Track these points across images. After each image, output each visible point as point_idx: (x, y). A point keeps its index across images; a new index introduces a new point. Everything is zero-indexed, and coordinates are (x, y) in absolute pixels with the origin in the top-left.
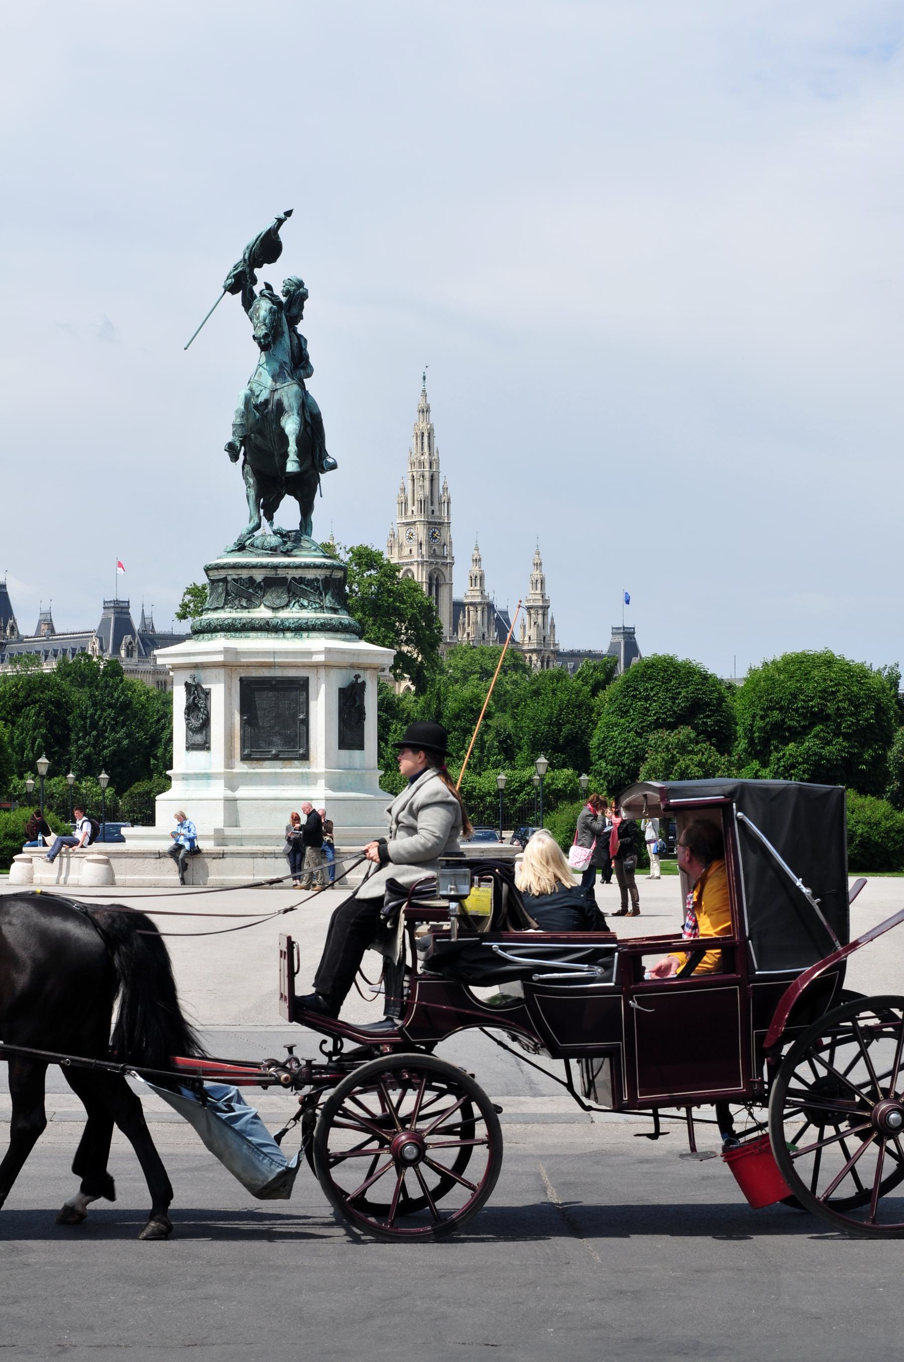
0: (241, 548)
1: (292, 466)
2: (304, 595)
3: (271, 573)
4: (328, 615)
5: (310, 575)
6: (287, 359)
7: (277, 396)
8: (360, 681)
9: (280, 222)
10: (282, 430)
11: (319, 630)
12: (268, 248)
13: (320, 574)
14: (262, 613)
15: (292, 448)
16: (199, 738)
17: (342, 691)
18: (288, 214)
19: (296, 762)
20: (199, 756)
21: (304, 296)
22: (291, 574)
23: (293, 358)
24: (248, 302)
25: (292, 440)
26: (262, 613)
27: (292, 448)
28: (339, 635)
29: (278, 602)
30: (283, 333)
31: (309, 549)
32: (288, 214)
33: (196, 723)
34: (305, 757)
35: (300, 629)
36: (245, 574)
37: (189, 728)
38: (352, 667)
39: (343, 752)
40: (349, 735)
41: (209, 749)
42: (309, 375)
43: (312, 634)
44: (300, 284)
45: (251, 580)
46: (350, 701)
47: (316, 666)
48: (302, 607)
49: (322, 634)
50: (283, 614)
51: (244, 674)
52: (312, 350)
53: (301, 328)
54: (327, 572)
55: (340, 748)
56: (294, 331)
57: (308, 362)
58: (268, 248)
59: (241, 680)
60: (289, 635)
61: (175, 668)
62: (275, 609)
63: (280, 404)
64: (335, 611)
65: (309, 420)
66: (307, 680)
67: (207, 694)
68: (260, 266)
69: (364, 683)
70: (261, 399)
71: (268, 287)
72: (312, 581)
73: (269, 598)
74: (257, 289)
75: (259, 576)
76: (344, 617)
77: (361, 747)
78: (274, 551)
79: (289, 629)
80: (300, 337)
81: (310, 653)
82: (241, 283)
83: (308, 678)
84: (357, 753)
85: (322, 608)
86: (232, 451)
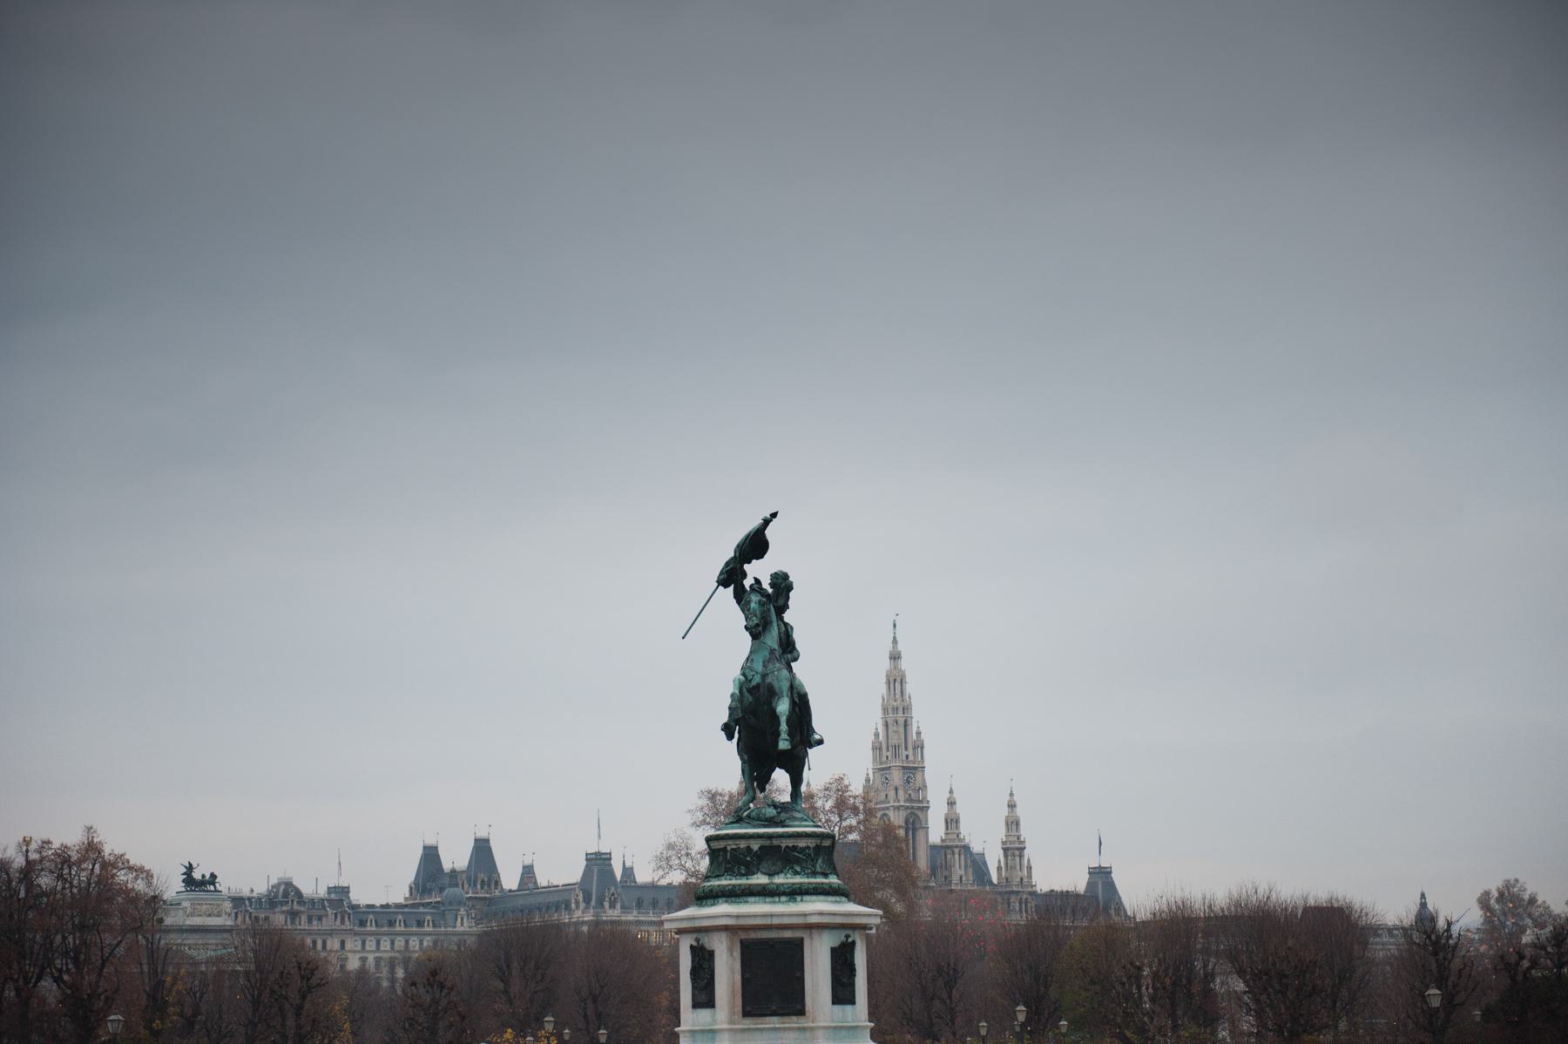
0: (739, 820)
1: (783, 745)
2: (798, 861)
3: (767, 843)
4: (820, 880)
5: (802, 843)
6: (776, 646)
7: (769, 680)
9: (766, 522)
10: (774, 711)
12: (755, 545)
13: (811, 843)
14: (760, 879)
15: (784, 727)
16: (703, 998)
17: (833, 950)
18: (774, 515)
20: (704, 1015)
21: (790, 588)
22: (784, 843)
23: (781, 645)
24: (740, 595)
25: (783, 720)
26: (760, 879)
27: (784, 727)
28: (830, 898)
31: (802, 819)
32: (774, 515)
33: (703, 984)
34: (801, 1012)
35: (794, 893)
36: (743, 844)
37: (694, 988)
38: (843, 926)
39: (837, 1007)
40: (842, 993)
41: (713, 1006)
42: (795, 659)
43: (806, 898)
44: (785, 576)
45: (749, 849)
46: (842, 960)
47: (810, 927)
48: (796, 873)
49: (814, 898)
50: (779, 880)
51: (744, 936)
52: (796, 636)
53: (787, 617)
56: (782, 619)
57: (794, 648)
58: (755, 545)
59: (742, 942)
60: (783, 899)
61: (680, 931)
62: (770, 875)
64: (825, 875)
66: (802, 940)
67: (711, 954)
69: (854, 943)
70: (754, 683)
71: (757, 581)
72: (803, 849)
73: (764, 866)
74: (748, 583)
75: (755, 846)
77: (851, 1001)
78: (771, 822)
79: (784, 894)
80: (786, 624)
81: (805, 915)
82: (731, 576)
84: (849, 1008)
85: (814, 874)
86: (728, 730)
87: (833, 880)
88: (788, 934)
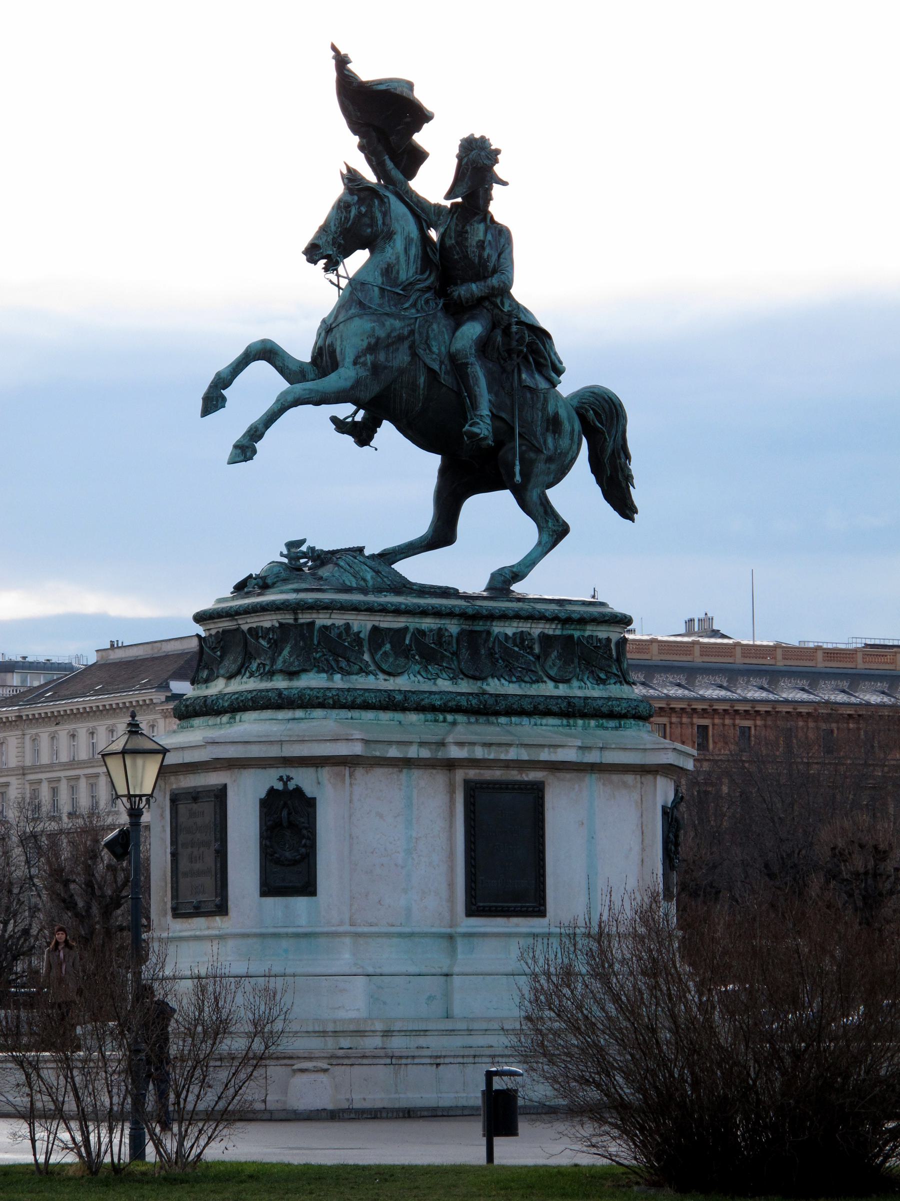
4: (280, 683)
8: (291, 786)
9: (342, 62)
11: (254, 709)
14: (218, 687)
17: (264, 803)
18: (334, 48)
19: (218, 918)
26: (218, 687)
29: (234, 668)
30: (389, 236)
32: (334, 48)
39: (270, 901)
54: (288, 618)
55: (263, 894)
60: (225, 718)
63: (332, 353)
64: (292, 675)
65: (436, 367)
68: (418, 129)
69: (298, 791)
72: (268, 630)
76: (312, 681)
77: (308, 888)
83: (225, 786)
84: (300, 903)
85: (271, 674)
87: (312, 681)
88: (213, 779)
